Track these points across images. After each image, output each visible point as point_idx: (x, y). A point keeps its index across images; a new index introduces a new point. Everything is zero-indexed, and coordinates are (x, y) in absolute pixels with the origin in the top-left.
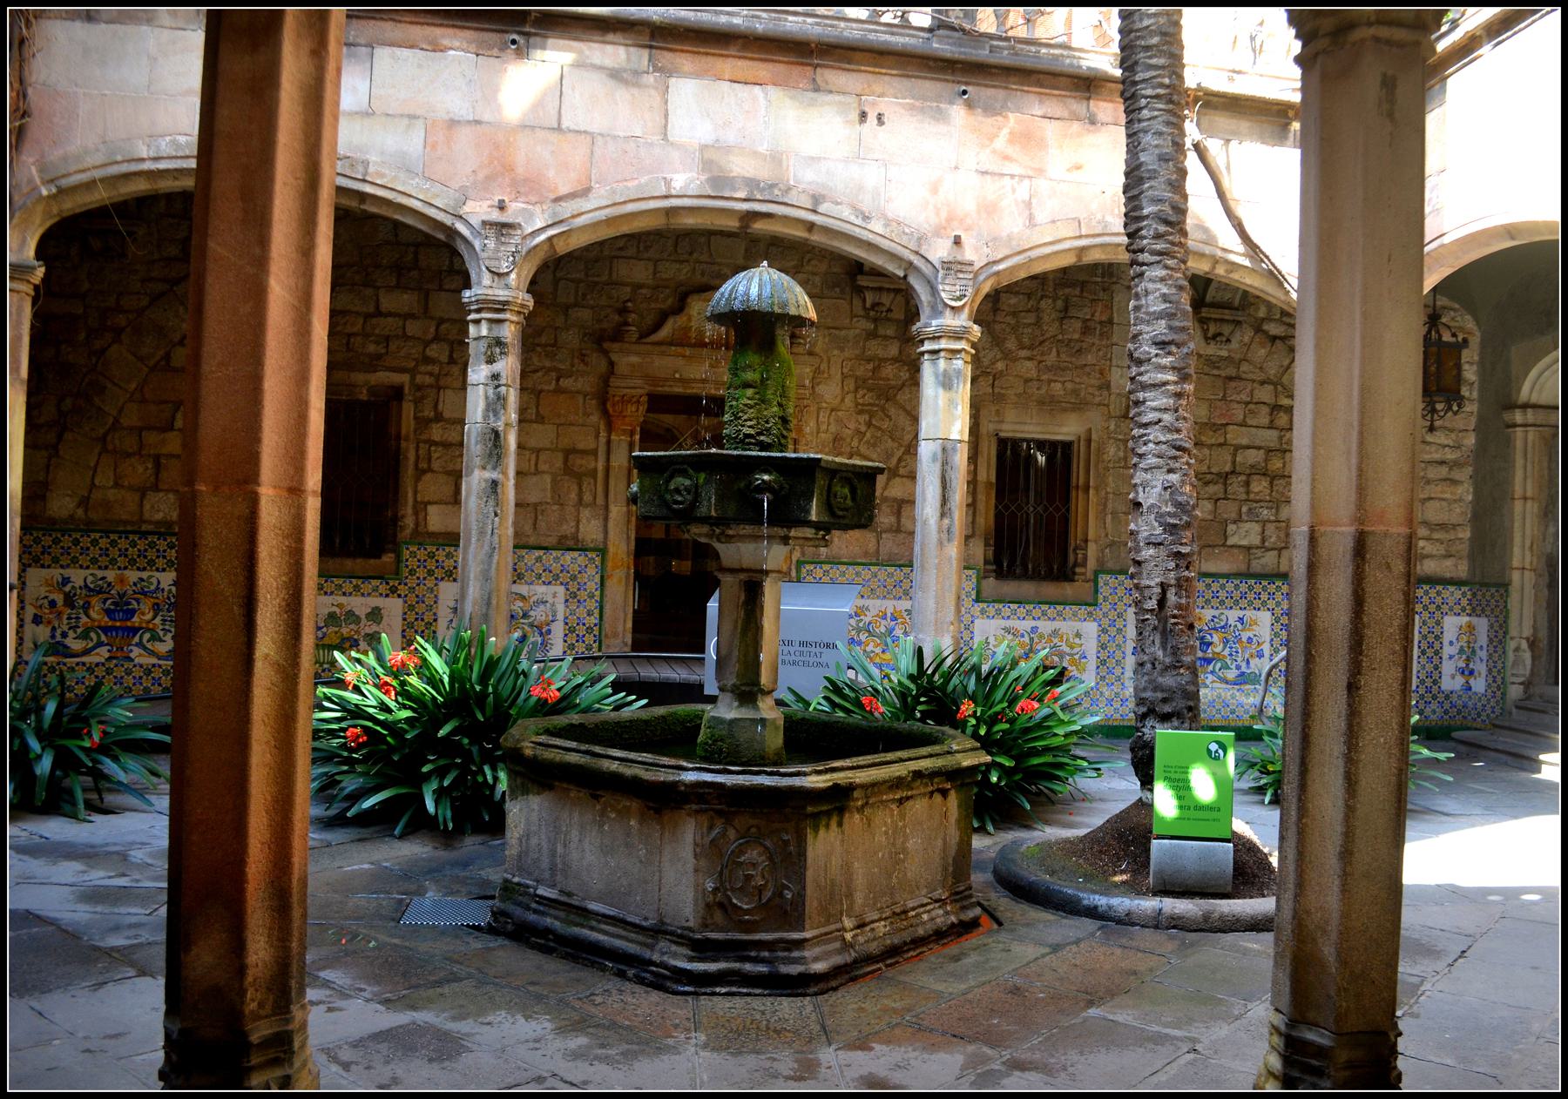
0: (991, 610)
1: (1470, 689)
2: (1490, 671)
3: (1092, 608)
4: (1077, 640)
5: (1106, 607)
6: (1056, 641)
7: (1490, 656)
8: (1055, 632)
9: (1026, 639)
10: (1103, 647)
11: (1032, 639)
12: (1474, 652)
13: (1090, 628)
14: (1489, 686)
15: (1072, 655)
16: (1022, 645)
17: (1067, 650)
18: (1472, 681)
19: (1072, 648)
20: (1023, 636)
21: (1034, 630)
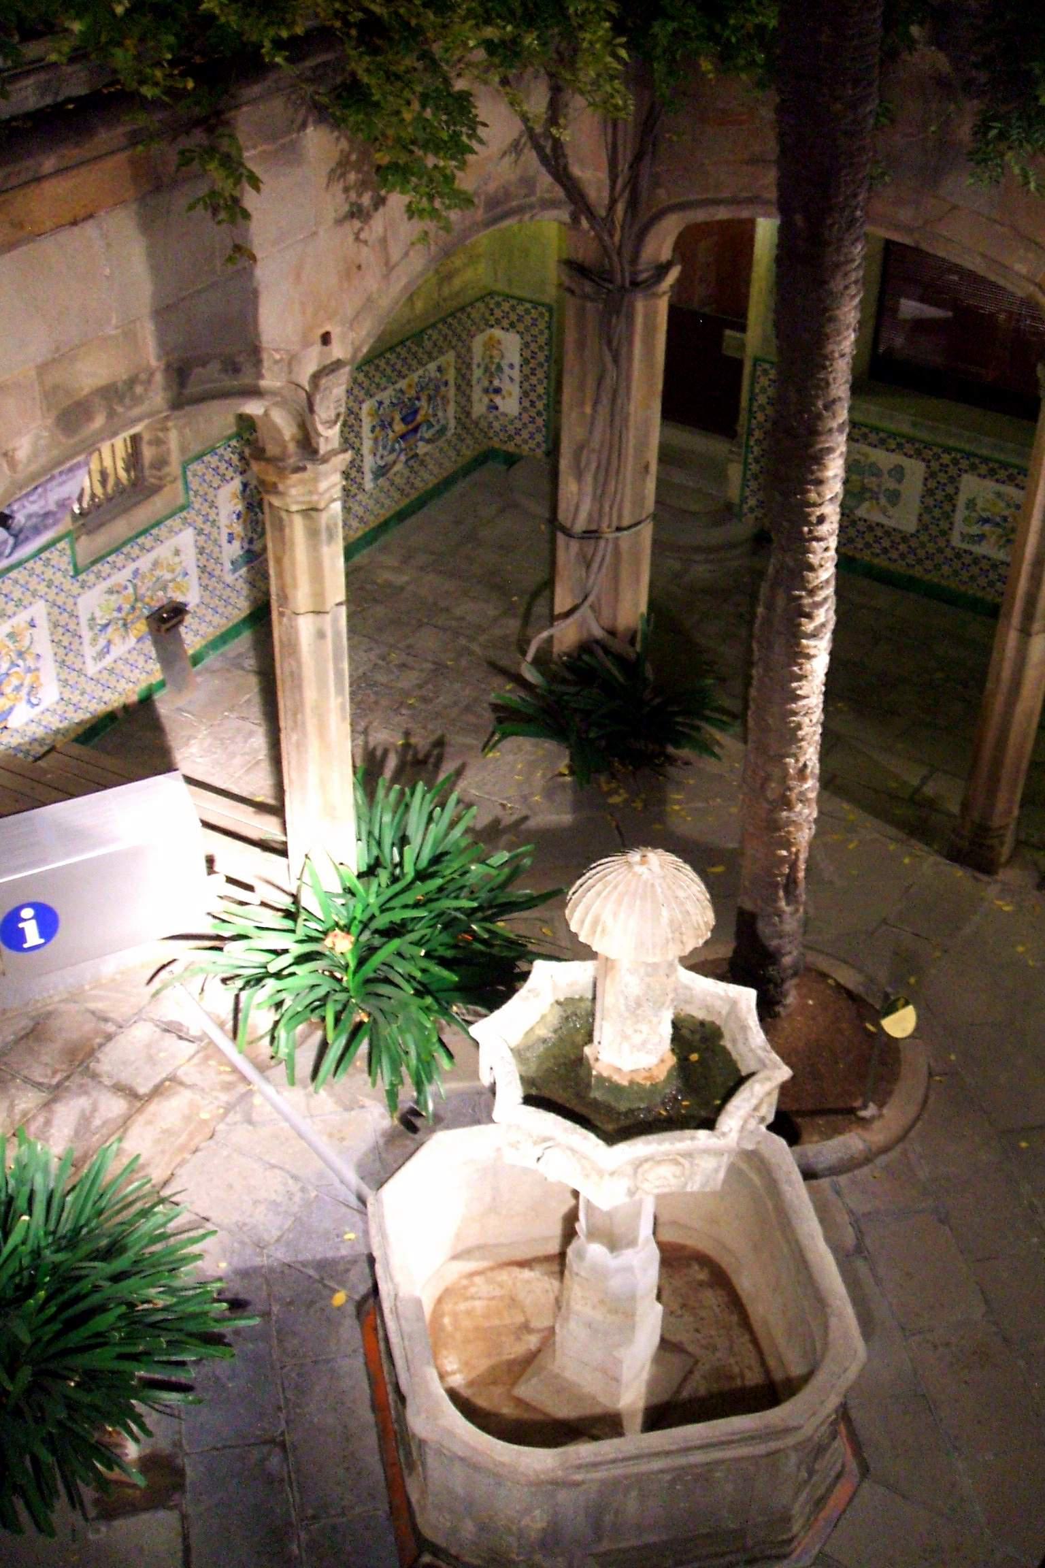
0: (91, 578)
1: (497, 408)
2: (526, 394)
3: (184, 514)
4: (177, 559)
5: (197, 503)
6: (158, 573)
7: (526, 378)
8: (156, 564)
9: (131, 590)
10: (201, 551)
11: (135, 587)
12: (499, 368)
13: (187, 538)
14: (525, 409)
15: (173, 580)
16: (126, 598)
17: (168, 576)
18: (498, 400)
19: (173, 571)
20: (126, 588)
21: (136, 572)
